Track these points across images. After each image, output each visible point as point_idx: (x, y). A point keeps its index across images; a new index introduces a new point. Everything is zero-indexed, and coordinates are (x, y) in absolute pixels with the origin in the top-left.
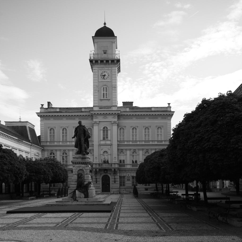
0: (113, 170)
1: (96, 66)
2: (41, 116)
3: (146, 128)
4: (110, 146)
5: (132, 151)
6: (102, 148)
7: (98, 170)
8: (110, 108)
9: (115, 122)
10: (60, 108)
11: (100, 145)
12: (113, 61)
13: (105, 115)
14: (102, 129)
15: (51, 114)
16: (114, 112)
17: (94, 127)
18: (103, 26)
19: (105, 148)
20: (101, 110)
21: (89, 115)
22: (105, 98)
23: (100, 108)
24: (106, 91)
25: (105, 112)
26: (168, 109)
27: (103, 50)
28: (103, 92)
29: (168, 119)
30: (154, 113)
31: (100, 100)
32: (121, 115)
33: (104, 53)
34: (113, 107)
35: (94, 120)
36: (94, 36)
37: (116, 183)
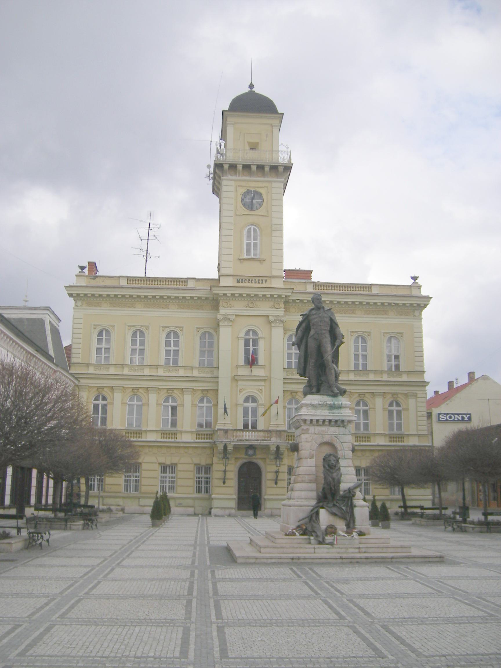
0: (273, 448)
1: (230, 177)
2: (78, 295)
3: (358, 337)
4: (263, 383)
7: (230, 448)
8: (264, 282)
9: (278, 320)
10: (129, 279)
11: (235, 379)
12: (274, 168)
13: (252, 299)
14: (242, 334)
15: (104, 292)
16: (276, 293)
17: (222, 329)
18: (247, 90)
19: (251, 389)
20: (240, 285)
21: (207, 298)
22: (252, 256)
23: (238, 281)
24: (255, 239)
25: (252, 292)
26: (415, 293)
27: (249, 143)
28: (245, 242)
29: (415, 316)
30: (379, 301)
31: (240, 259)
32: (294, 301)
33: (252, 149)
34: (273, 280)
35: (222, 311)
36: (227, 108)
37: (280, 484)
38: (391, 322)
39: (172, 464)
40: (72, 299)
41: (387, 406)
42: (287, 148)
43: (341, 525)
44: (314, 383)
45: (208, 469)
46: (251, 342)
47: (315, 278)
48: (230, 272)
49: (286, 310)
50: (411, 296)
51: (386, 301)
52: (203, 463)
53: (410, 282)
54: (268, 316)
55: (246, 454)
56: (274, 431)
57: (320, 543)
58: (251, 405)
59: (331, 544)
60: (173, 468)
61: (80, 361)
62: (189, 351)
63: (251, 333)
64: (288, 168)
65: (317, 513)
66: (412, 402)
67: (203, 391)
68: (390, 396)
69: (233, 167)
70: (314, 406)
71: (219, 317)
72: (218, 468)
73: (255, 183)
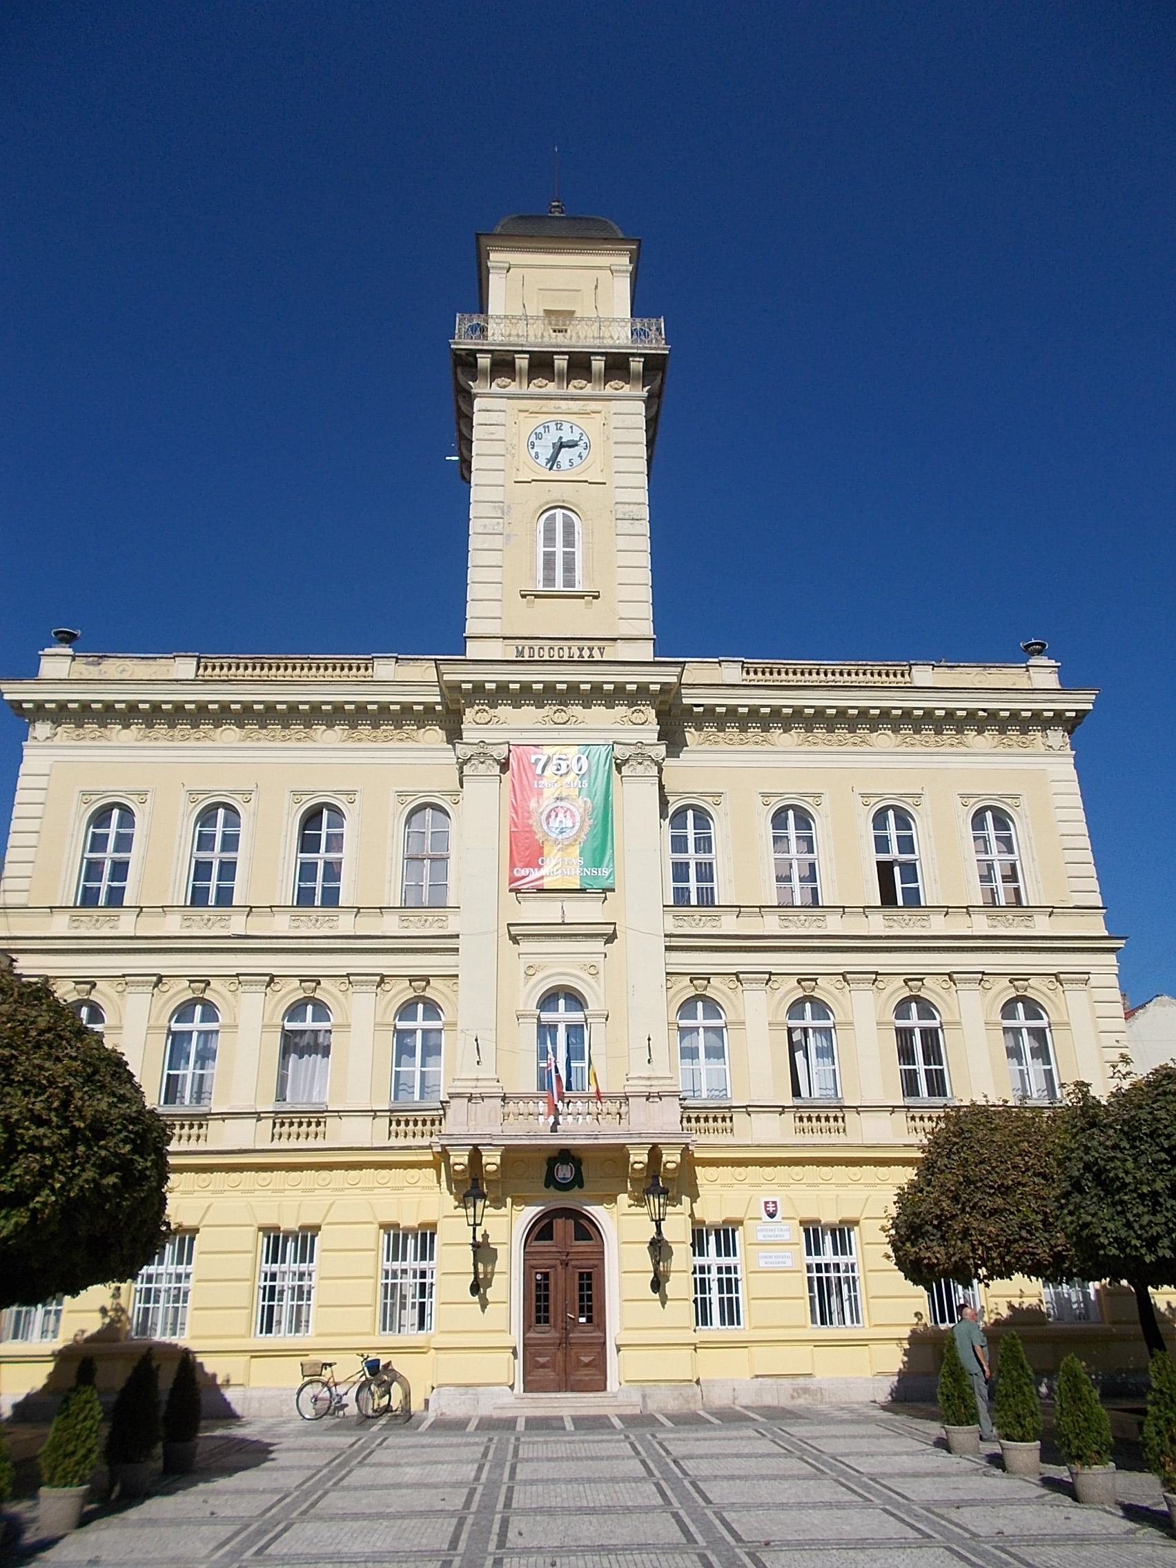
0: (639, 1157)
4: (599, 945)
5: (783, 990)
6: (532, 960)
7: (491, 1159)
19: (563, 964)
22: (559, 586)
24: (569, 542)
28: (541, 550)
39: (302, 1228)
52: (409, 1220)
58: (562, 1015)
60: (306, 1238)
68: (1005, 981)
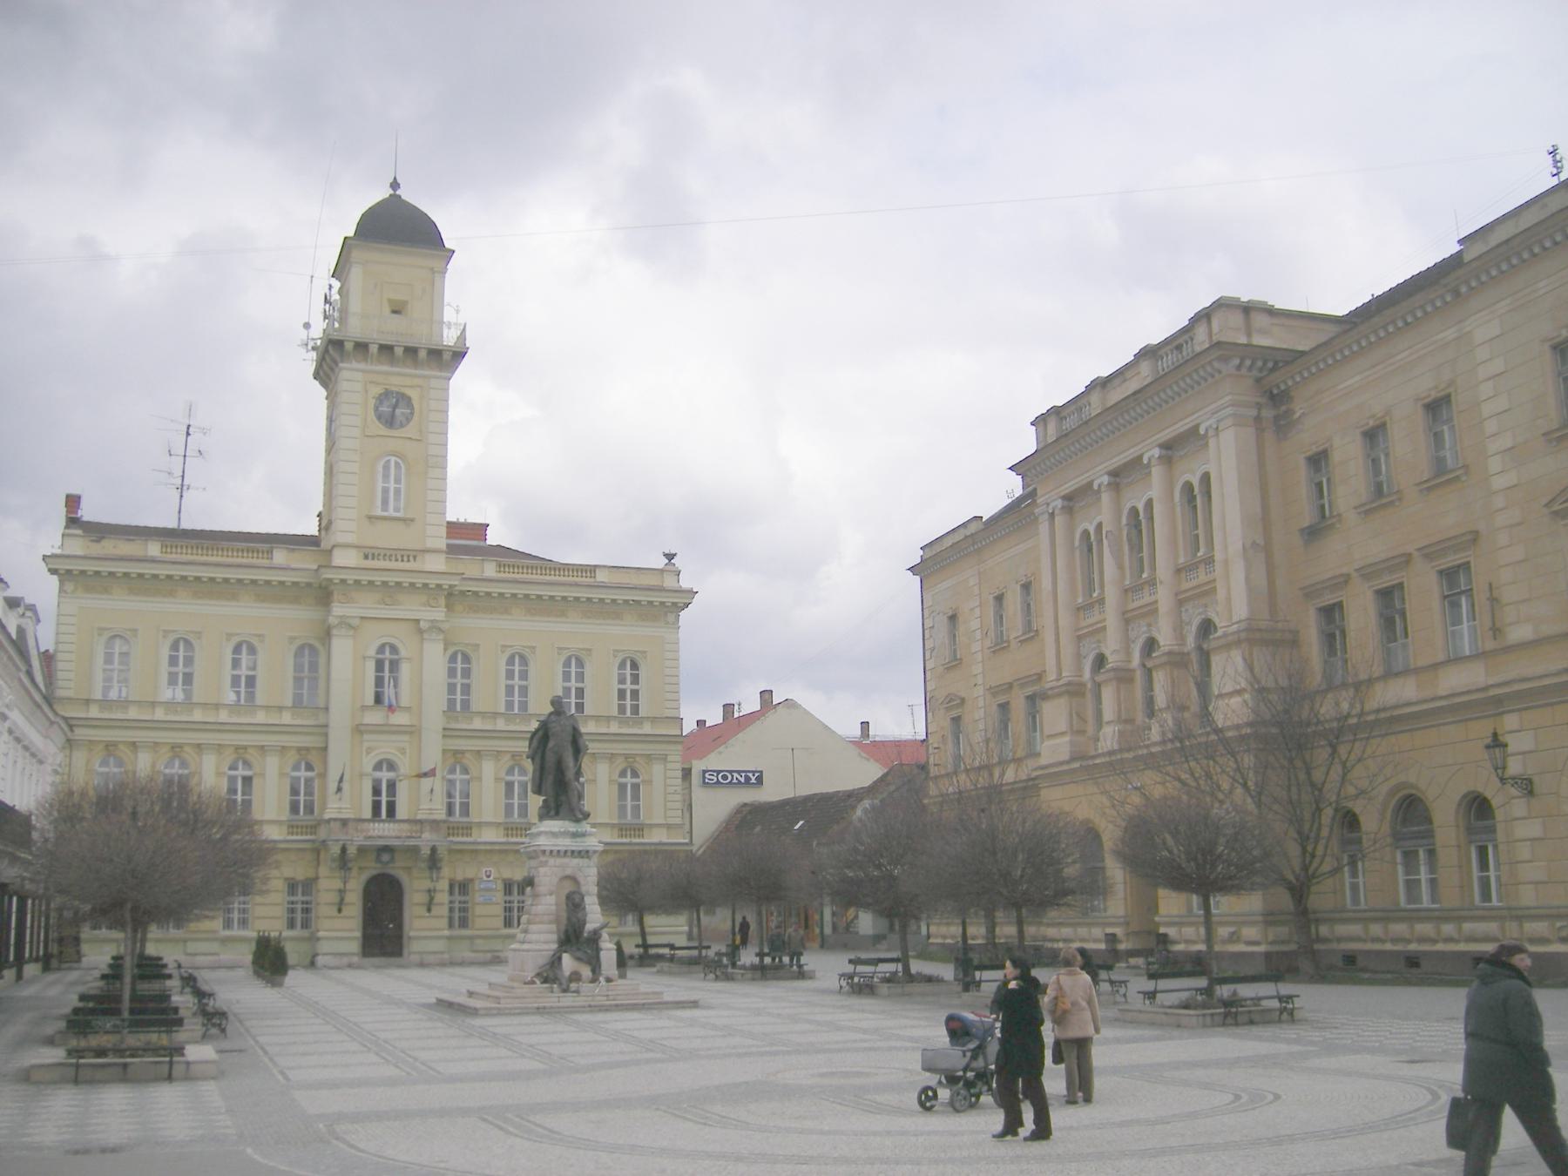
0: (426, 851)
1: (355, 365)
2: (69, 572)
3: (569, 659)
4: (406, 738)
7: (352, 850)
9: (435, 627)
11: (359, 730)
12: (436, 354)
13: (390, 591)
14: (372, 652)
15: (120, 568)
16: (433, 582)
19: (386, 747)
20: (370, 563)
21: (309, 585)
22: (391, 512)
23: (366, 557)
24: (397, 481)
25: (392, 579)
26: (669, 582)
27: (390, 301)
28: (380, 485)
30: (608, 596)
31: (370, 518)
32: (463, 593)
33: (394, 312)
34: (427, 556)
35: (338, 610)
37: (435, 911)
38: (627, 634)
40: (55, 577)
41: (615, 777)
42: (458, 312)
43: (586, 972)
44: (552, 805)
45: (309, 885)
46: (387, 665)
47: (493, 538)
48: (350, 539)
49: (449, 607)
50: (662, 589)
51: (621, 596)
53: (661, 562)
54: (418, 621)
55: (378, 860)
56: (426, 821)
57: (565, 991)
58: (385, 775)
59: (577, 992)
61: (70, 693)
62: (276, 677)
63: (387, 650)
64: (459, 354)
65: (560, 959)
66: (657, 769)
67: (299, 749)
69: (362, 347)
70: (554, 835)
71: (332, 620)
72: (328, 884)
73: (401, 378)
